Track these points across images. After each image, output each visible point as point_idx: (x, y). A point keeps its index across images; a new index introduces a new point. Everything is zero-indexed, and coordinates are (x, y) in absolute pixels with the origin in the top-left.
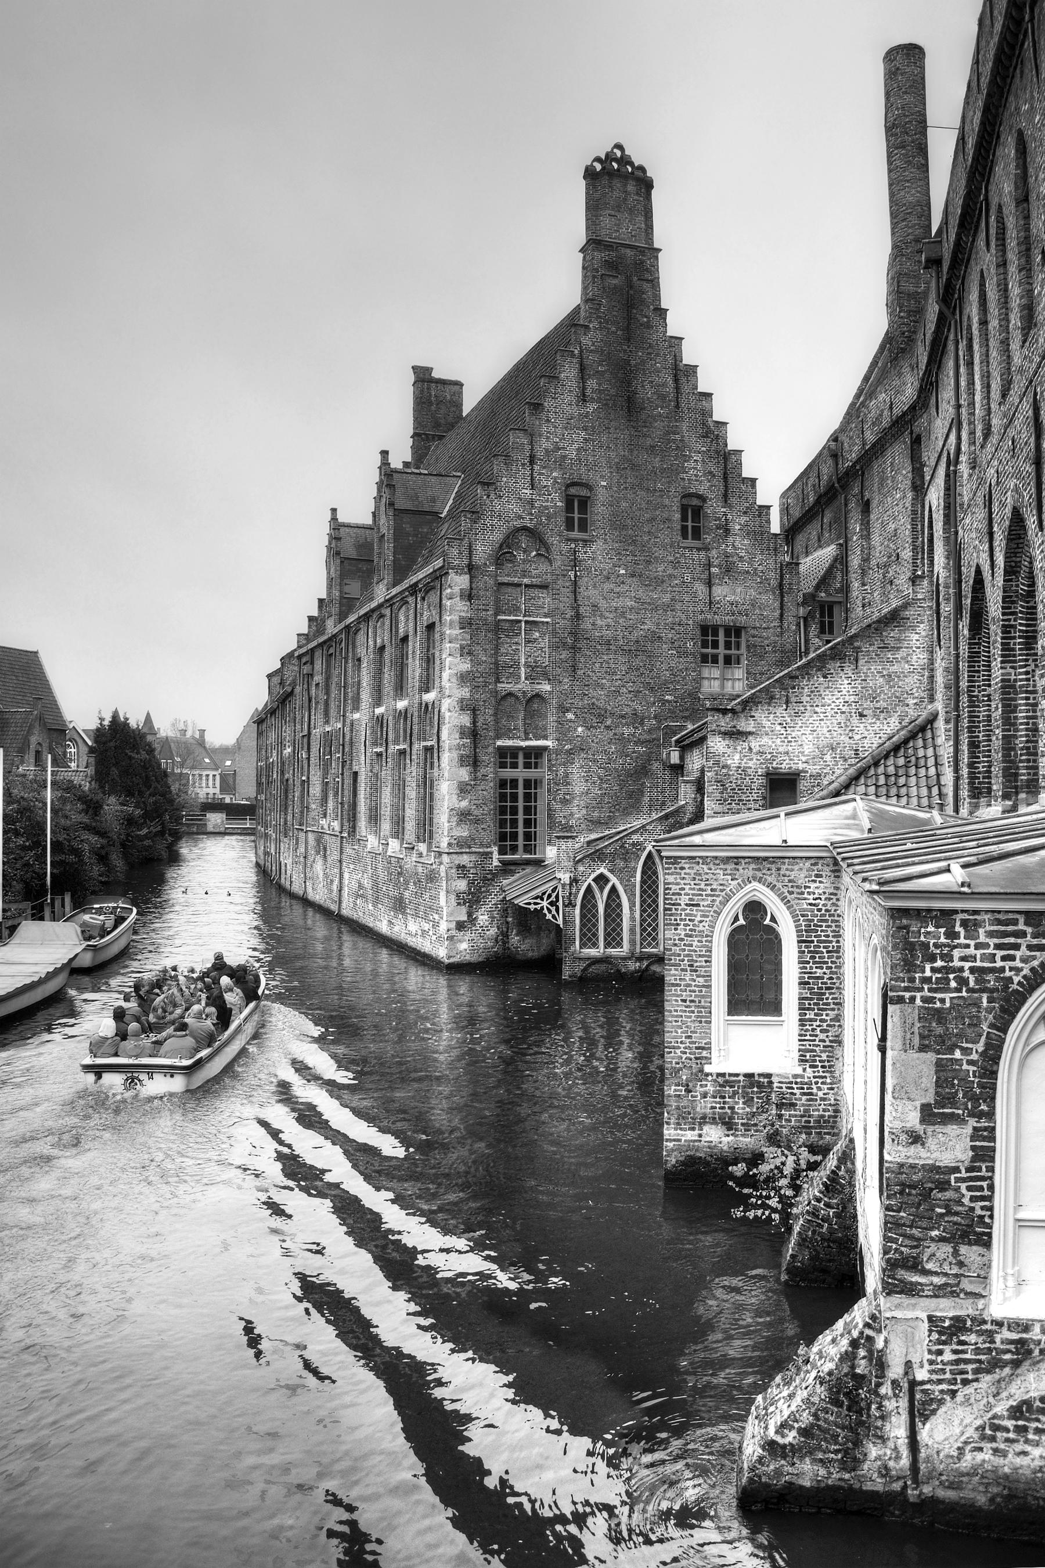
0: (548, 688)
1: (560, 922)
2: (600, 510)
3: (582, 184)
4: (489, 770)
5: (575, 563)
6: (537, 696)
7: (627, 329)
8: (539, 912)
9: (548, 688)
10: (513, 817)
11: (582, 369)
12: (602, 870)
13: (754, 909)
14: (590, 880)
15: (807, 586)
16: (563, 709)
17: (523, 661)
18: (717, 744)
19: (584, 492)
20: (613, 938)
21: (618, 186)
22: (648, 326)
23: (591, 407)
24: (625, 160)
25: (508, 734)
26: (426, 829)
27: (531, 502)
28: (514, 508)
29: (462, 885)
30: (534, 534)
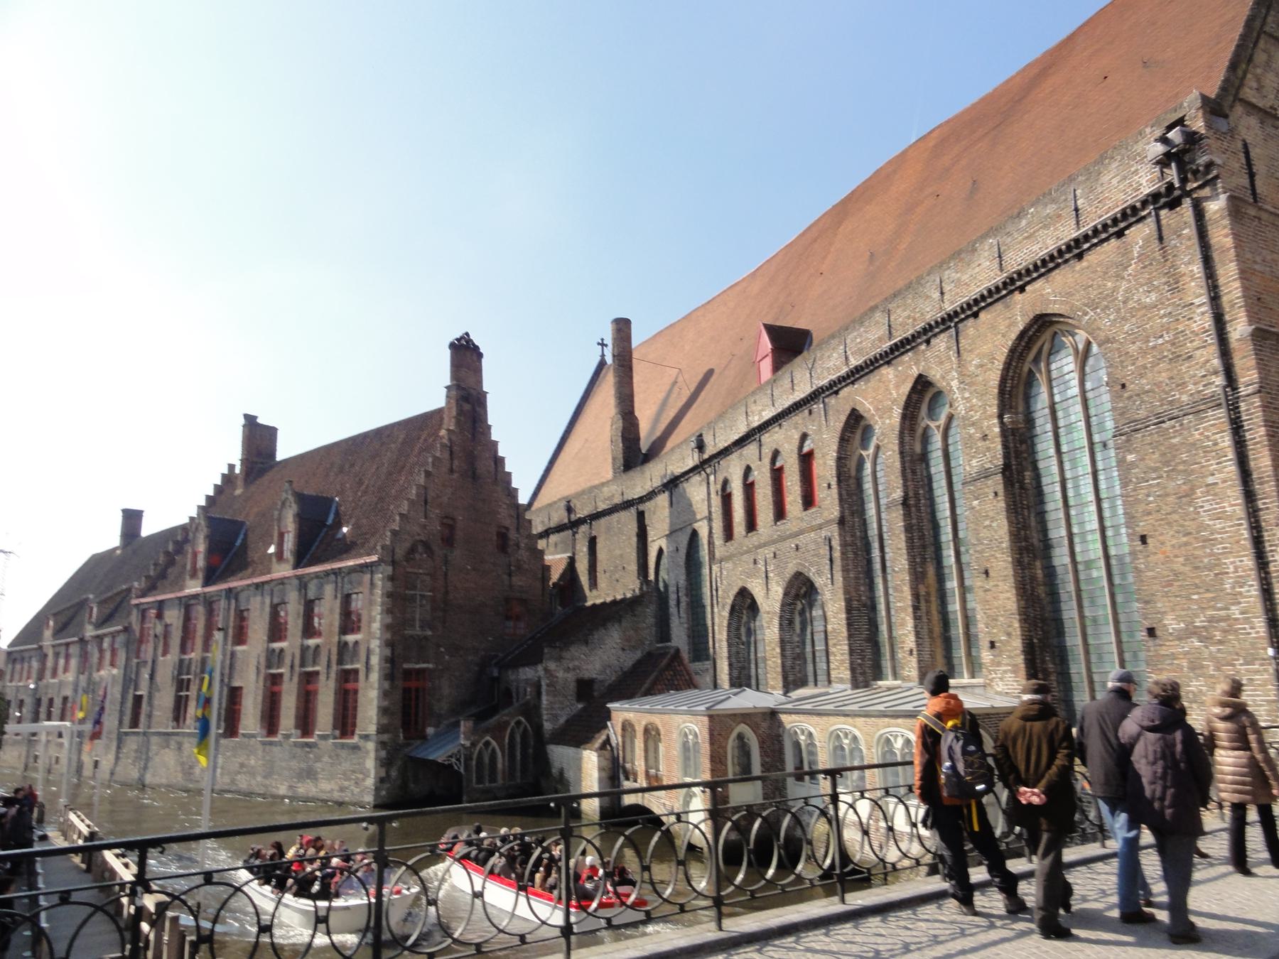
0: (430, 633)
1: (462, 770)
2: (459, 534)
3: (448, 352)
4: (400, 683)
5: (446, 562)
6: (426, 638)
7: (473, 435)
8: (451, 766)
9: (430, 633)
10: (409, 710)
11: (451, 453)
12: (488, 738)
13: (740, 737)
14: (481, 745)
15: (555, 576)
16: (439, 646)
17: (417, 616)
18: (552, 665)
19: (451, 522)
20: (493, 780)
21: (465, 354)
22: (483, 433)
23: (455, 476)
24: (469, 341)
25: (407, 660)
26: (345, 722)
27: (424, 527)
28: (416, 529)
29: (383, 754)
30: (427, 546)
